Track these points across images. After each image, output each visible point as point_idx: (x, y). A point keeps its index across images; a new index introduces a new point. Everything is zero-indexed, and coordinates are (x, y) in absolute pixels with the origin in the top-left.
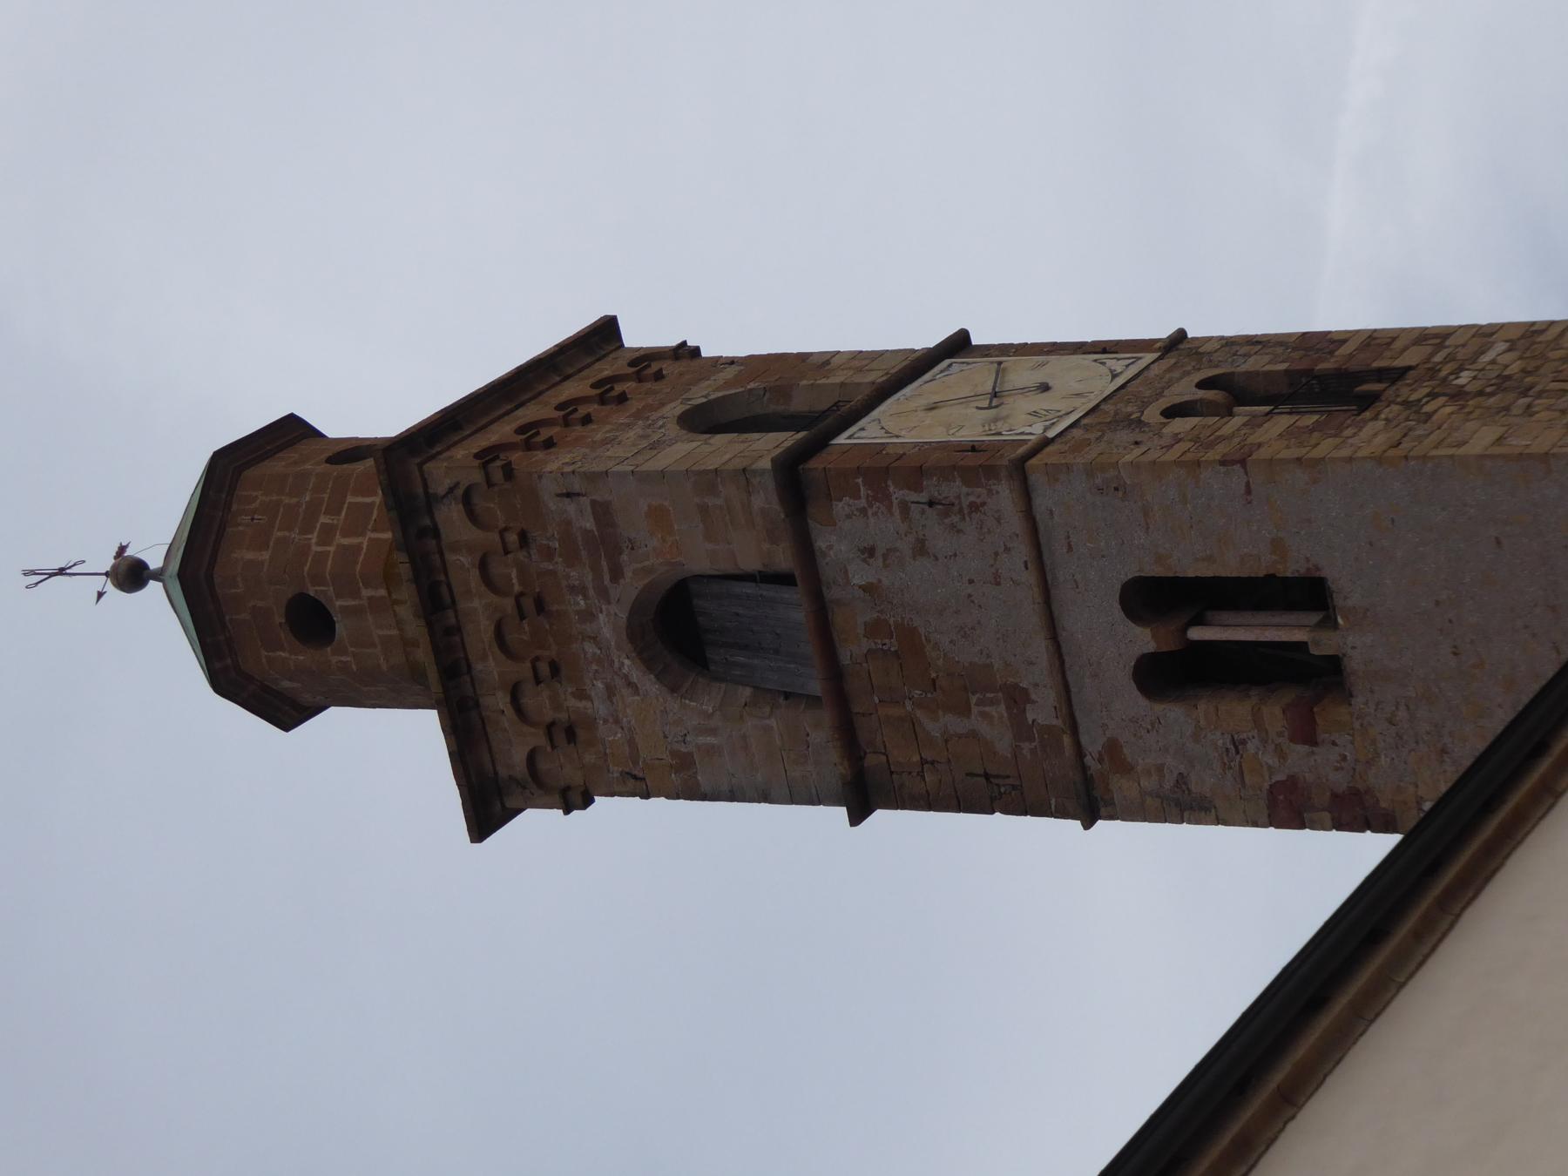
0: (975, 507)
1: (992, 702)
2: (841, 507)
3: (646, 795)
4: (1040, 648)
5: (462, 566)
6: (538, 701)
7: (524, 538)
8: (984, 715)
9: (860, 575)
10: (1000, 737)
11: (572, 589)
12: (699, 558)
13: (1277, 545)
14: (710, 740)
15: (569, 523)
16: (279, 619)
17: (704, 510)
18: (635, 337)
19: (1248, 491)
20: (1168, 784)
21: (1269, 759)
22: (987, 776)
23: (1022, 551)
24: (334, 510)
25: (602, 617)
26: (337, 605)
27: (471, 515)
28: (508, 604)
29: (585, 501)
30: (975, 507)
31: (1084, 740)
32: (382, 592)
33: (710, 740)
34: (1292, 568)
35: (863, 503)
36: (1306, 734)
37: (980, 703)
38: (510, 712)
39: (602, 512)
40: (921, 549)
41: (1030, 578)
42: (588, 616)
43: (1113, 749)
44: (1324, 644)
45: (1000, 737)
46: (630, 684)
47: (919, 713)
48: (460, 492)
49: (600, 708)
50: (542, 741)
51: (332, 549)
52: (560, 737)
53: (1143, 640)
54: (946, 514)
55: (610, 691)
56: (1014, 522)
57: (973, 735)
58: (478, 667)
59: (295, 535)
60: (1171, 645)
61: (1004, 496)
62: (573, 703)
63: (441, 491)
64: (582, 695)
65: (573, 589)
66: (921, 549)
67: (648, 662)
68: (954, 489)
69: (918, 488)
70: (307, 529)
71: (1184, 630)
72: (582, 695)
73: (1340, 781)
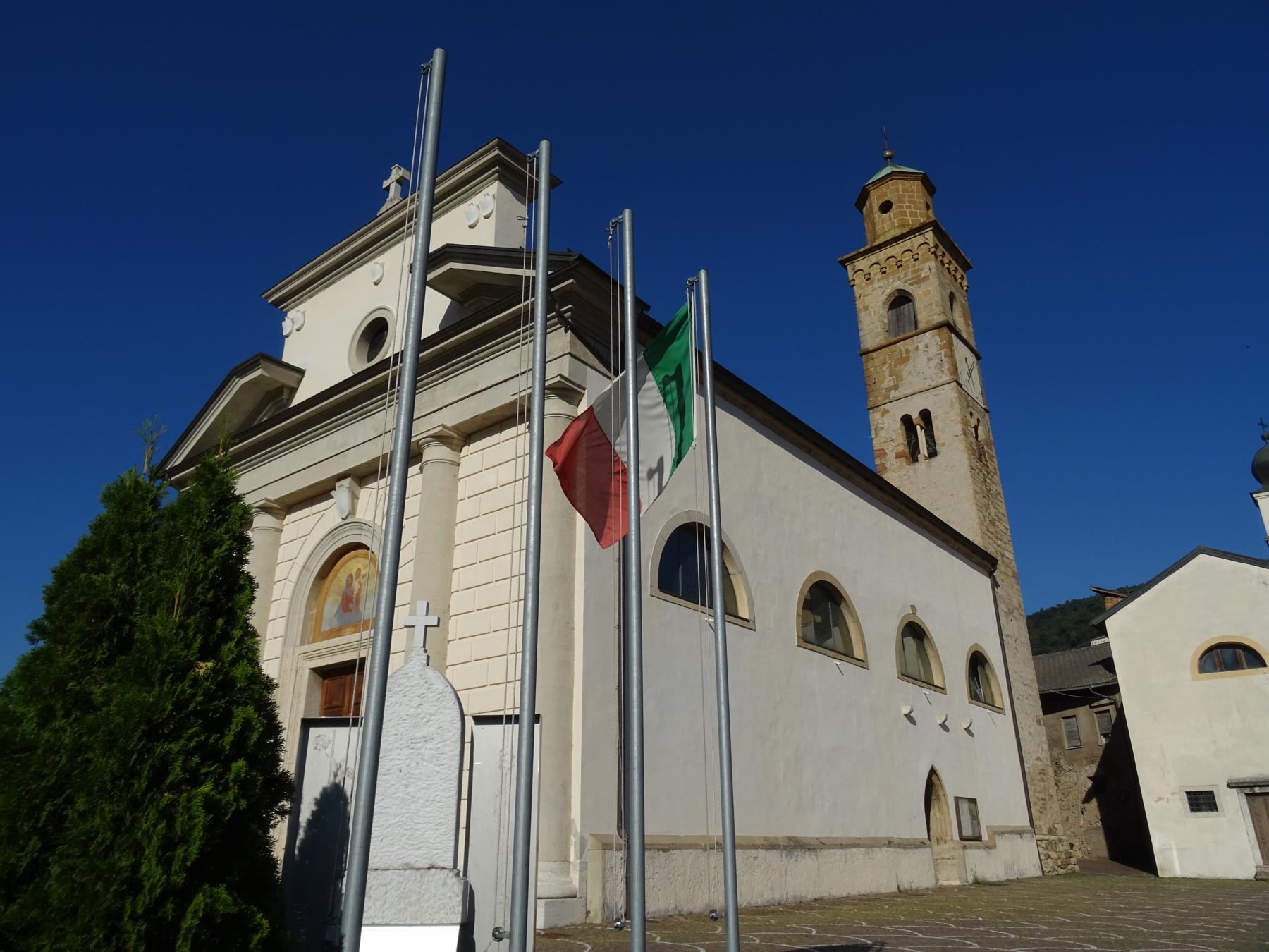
0: (942, 371)
1: (894, 382)
2: (937, 338)
4: (909, 391)
5: (907, 244)
7: (917, 259)
8: (890, 381)
9: (921, 346)
10: (886, 384)
11: (906, 274)
13: (943, 444)
14: (873, 315)
15: (922, 270)
19: (957, 436)
20: (881, 426)
21: (890, 449)
22: (875, 383)
23: (933, 384)
24: (915, 207)
25: (899, 282)
26: (891, 213)
28: (899, 259)
29: (929, 273)
31: (888, 404)
32: (896, 225)
33: (873, 315)
34: (938, 448)
35: (939, 343)
36: (898, 456)
37: (893, 379)
38: (872, 263)
40: (930, 359)
41: (927, 387)
42: (899, 278)
43: (887, 412)
44: (920, 457)
45: (886, 384)
47: (887, 365)
48: (927, 241)
49: (876, 285)
50: (866, 272)
51: (905, 209)
52: (867, 276)
53: (915, 416)
54: (940, 364)
55: (881, 287)
56: (940, 381)
57: (885, 378)
59: (907, 199)
60: (915, 422)
62: (876, 279)
63: (926, 236)
64: (879, 280)
66: (930, 359)
68: (946, 366)
70: (909, 202)
71: (919, 425)
72: (879, 280)
73: (888, 465)
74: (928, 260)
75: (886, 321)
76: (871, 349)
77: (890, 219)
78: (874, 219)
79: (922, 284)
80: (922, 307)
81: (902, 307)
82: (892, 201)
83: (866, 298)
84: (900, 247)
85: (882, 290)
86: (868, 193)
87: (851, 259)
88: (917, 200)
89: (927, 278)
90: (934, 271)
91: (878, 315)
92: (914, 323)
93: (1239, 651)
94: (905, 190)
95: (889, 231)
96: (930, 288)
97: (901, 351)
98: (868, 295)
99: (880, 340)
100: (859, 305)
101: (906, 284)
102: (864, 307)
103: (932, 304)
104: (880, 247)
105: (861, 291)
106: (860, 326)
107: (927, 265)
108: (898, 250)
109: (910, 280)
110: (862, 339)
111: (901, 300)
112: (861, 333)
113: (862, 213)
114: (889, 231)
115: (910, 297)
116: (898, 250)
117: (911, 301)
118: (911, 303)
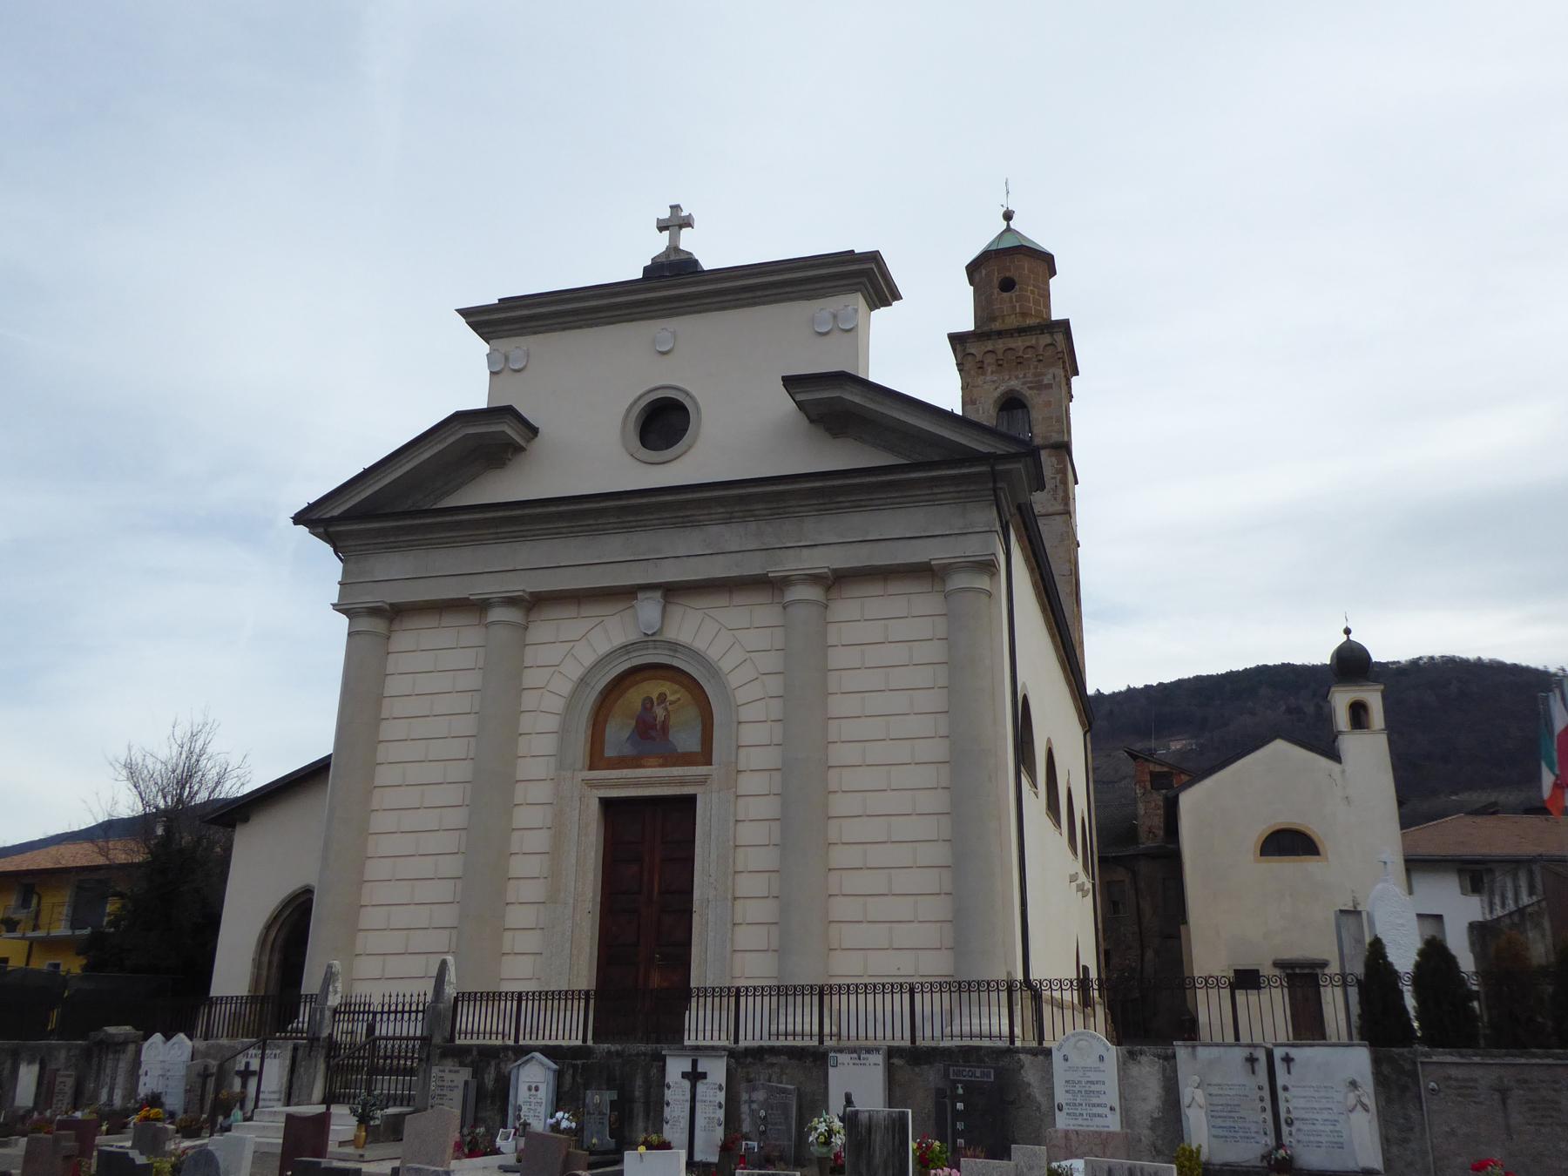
0: (1055, 499)
2: (1054, 459)
3: (962, 388)
6: (990, 359)
7: (1041, 360)
12: (1036, 415)
14: (981, 412)
15: (1045, 375)
16: (1007, 275)
18: (1074, 380)
19: (1064, 575)
26: (1013, 294)
27: (1046, 346)
28: (1020, 354)
30: (1055, 499)
33: (981, 412)
38: (986, 350)
39: (1049, 386)
42: (1017, 378)
46: (996, 388)
50: (979, 358)
52: (979, 365)
55: (994, 381)
56: (1051, 510)
58: (1000, 341)
61: (1059, 507)
62: (990, 370)
63: (1055, 337)
64: (992, 373)
65: (1025, 374)
67: (1003, 395)
68: (1061, 494)
70: (1034, 286)
72: (992, 373)
80: (1040, 418)
82: (1016, 279)
95: (1009, 315)
98: (978, 386)
101: (1025, 387)
109: (1031, 382)
114: (1009, 315)
118: (1025, 410)
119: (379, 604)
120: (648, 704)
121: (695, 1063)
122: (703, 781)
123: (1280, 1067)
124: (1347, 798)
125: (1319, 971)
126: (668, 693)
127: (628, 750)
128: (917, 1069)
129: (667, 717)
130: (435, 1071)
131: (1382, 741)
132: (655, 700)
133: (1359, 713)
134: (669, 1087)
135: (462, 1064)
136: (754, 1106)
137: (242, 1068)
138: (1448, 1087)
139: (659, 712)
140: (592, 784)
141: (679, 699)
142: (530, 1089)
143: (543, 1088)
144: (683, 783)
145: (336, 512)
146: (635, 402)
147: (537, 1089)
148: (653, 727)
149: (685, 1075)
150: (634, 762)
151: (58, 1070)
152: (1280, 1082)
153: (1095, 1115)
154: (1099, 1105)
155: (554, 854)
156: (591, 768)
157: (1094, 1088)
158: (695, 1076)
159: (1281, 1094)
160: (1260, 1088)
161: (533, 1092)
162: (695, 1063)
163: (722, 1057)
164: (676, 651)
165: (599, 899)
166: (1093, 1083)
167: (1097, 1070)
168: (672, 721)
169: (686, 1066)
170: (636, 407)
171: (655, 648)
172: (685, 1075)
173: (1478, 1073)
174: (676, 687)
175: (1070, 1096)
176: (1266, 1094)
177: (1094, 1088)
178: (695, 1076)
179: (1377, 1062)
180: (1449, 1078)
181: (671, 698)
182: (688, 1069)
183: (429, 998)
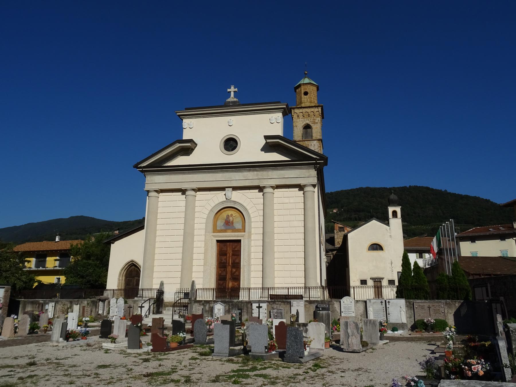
5: (312, 110)
9: (313, 144)
15: (316, 120)
16: (306, 91)
17: (317, 132)
25: (308, 121)
26: (307, 96)
28: (309, 114)
32: (309, 101)
38: (300, 112)
42: (308, 120)
49: (301, 120)
55: (302, 121)
58: (304, 110)
59: (312, 93)
64: (302, 118)
65: (311, 119)
69: (320, 150)
72: (302, 118)
74: (318, 117)
75: (302, 132)
76: (297, 141)
77: (307, 98)
78: (301, 96)
79: (315, 124)
80: (314, 132)
81: (308, 129)
82: (308, 92)
83: (297, 123)
84: (310, 110)
85: (302, 122)
86: (301, 86)
87: (294, 108)
88: (315, 94)
89: (317, 123)
90: (320, 121)
91: (300, 130)
92: (311, 136)
93: (378, 246)
94: (312, 90)
95: (306, 102)
96: (318, 127)
97: (306, 144)
98: (298, 122)
99: (300, 139)
100: (294, 124)
101: (310, 123)
102: (296, 126)
103: (317, 132)
104: (304, 108)
105: (295, 120)
106: (294, 132)
107: (318, 119)
108: (309, 111)
109: (312, 122)
110: (294, 136)
111: (307, 127)
112: (294, 134)
113: (295, 91)
114: (306, 102)
115: (310, 127)
116: (309, 111)
117: (310, 128)
118: (310, 129)
119: (157, 189)
120: (228, 216)
121: (259, 305)
122: (243, 236)
123: (387, 304)
124: (391, 236)
125: (381, 280)
126: (233, 214)
127: (223, 228)
128: (311, 305)
129: (233, 220)
130: (194, 306)
131: (400, 220)
132: (230, 216)
133: (395, 214)
134: (253, 310)
135: (200, 305)
136: (274, 313)
137: (140, 306)
138: (420, 307)
139: (231, 219)
140: (215, 236)
141: (236, 216)
142: (218, 310)
143: (222, 310)
144: (238, 237)
145: (145, 165)
146: (223, 138)
147: (220, 310)
148: (229, 222)
149: (257, 307)
150: (225, 231)
151: (85, 306)
152: (387, 306)
153: (350, 313)
154: (350, 311)
155: (205, 253)
156: (214, 232)
157: (350, 308)
158: (259, 307)
159: (387, 308)
160: (383, 308)
161: (219, 310)
162: (259, 305)
163: (266, 303)
164: (235, 203)
165: (216, 265)
166: (349, 307)
167: (350, 304)
168: (234, 221)
169: (257, 305)
170: (223, 139)
171: (230, 203)
172: (257, 307)
173: (425, 304)
174: (235, 212)
175: (344, 310)
176: (385, 309)
177: (350, 308)
178: (259, 307)
179: (406, 302)
180: (420, 305)
181: (234, 215)
182: (258, 306)
183: (190, 289)
